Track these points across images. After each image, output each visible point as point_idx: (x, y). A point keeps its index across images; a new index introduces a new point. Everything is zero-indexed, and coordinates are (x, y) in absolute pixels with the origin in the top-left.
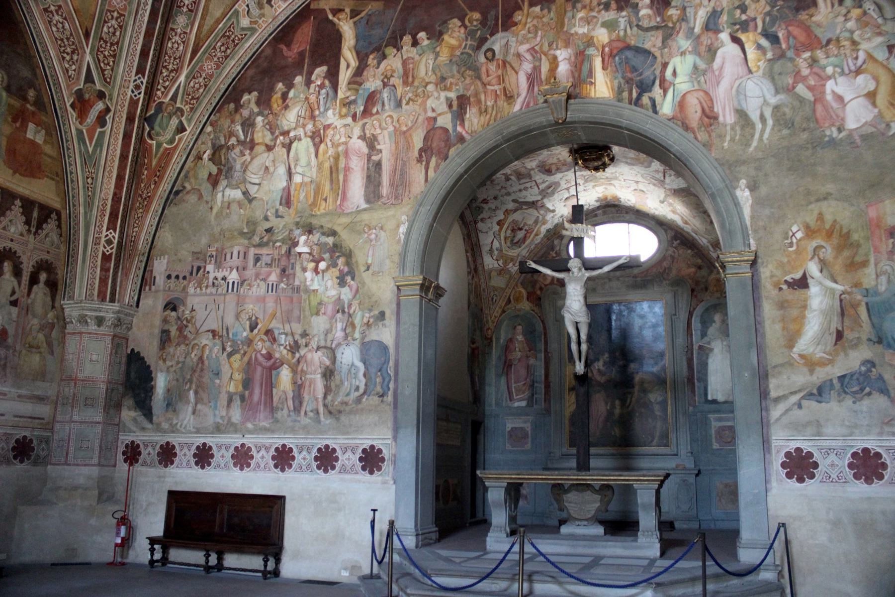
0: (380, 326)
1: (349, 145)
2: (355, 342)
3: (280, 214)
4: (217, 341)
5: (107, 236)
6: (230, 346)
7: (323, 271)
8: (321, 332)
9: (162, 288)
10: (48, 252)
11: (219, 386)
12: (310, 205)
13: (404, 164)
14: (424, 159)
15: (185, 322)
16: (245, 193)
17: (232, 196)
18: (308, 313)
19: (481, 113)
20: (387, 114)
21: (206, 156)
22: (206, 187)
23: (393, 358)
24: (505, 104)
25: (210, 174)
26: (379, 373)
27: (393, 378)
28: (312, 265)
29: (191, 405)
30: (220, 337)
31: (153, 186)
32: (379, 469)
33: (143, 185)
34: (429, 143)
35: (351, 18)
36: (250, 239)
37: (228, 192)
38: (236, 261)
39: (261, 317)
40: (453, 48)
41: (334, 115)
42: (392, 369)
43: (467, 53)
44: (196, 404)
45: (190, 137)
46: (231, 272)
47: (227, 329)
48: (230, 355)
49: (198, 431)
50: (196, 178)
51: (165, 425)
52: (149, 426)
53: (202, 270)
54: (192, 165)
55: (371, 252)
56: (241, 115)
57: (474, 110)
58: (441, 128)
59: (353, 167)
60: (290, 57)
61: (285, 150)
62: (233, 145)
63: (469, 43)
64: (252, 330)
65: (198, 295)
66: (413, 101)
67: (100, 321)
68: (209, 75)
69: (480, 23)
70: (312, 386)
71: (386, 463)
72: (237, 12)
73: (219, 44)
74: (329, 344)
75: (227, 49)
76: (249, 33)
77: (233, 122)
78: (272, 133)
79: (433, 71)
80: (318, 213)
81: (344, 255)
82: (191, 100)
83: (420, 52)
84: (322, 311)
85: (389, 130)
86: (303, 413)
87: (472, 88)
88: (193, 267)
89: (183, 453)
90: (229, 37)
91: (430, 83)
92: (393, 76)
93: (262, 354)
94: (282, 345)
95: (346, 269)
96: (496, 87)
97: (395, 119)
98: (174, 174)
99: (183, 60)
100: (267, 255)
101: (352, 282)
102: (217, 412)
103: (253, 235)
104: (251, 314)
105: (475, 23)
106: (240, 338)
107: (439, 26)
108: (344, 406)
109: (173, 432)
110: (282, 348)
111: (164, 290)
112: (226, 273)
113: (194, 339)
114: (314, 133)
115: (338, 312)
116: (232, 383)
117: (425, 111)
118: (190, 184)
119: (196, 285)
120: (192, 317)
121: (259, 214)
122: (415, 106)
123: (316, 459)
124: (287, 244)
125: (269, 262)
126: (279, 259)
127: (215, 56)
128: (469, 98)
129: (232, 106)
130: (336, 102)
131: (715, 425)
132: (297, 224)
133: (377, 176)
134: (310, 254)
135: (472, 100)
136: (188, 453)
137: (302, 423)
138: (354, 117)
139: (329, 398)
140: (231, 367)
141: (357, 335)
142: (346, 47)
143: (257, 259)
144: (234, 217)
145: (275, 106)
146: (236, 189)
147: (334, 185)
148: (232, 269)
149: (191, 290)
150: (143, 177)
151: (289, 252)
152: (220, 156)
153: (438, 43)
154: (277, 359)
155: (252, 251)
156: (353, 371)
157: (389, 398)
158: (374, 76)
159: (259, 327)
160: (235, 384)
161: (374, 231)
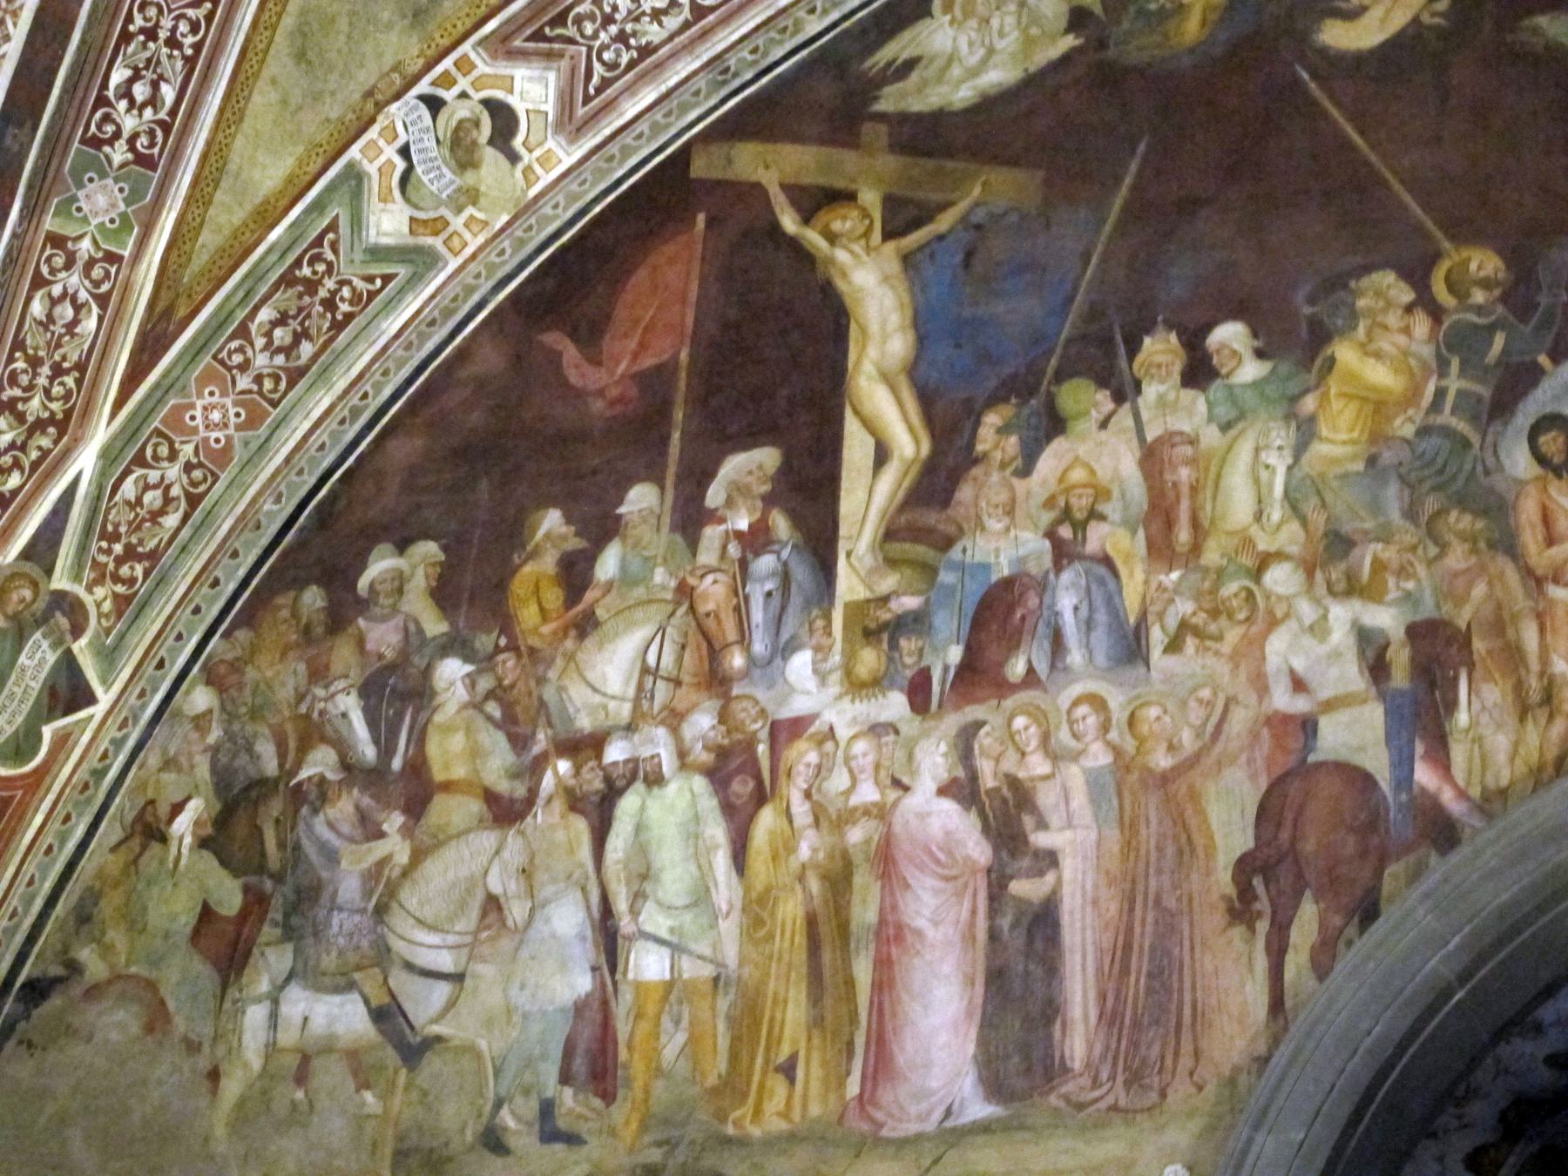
1: (897, 828)
3: (562, 1124)
12: (715, 1092)
13: (1168, 925)
14: (1263, 904)
16: (387, 1015)
17: (318, 1024)
19: (1524, 711)
20: (1077, 689)
21: (183, 826)
25: (207, 914)
34: (1285, 835)
35: (888, 235)
37: (297, 1003)
40: (1378, 406)
41: (821, 676)
43: (1447, 432)
45: (112, 732)
50: (135, 923)
54: (114, 864)
56: (361, 642)
57: (1494, 693)
59: (921, 923)
60: (600, 393)
61: (581, 827)
62: (322, 781)
63: (1454, 384)
66: (1198, 632)
68: (210, 452)
69: (1504, 299)
72: (354, 175)
73: (265, 315)
75: (297, 338)
76: (402, 271)
77: (319, 673)
78: (519, 742)
79: (1292, 502)
80: (755, 1131)
82: (119, 561)
83: (1224, 412)
85: (1088, 763)
87: (1479, 590)
90: (312, 286)
91: (1279, 556)
92: (1102, 518)
97: (1119, 714)
98: (28, 901)
99: (95, 385)
105: (1479, 297)
107: (1312, 300)
114: (722, 753)
117: (1261, 685)
118: (106, 950)
122: (1210, 660)
127: (244, 367)
128: (1464, 640)
129: (313, 598)
130: (828, 618)
133: (1037, 971)
135: (1479, 645)
138: (918, 692)
142: (868, 367)
144: (333, 1128)
145: (528, 615)
146: (337, 990)
147: (828, 1001)
153: (1312, 378)
158: (1010, 510)
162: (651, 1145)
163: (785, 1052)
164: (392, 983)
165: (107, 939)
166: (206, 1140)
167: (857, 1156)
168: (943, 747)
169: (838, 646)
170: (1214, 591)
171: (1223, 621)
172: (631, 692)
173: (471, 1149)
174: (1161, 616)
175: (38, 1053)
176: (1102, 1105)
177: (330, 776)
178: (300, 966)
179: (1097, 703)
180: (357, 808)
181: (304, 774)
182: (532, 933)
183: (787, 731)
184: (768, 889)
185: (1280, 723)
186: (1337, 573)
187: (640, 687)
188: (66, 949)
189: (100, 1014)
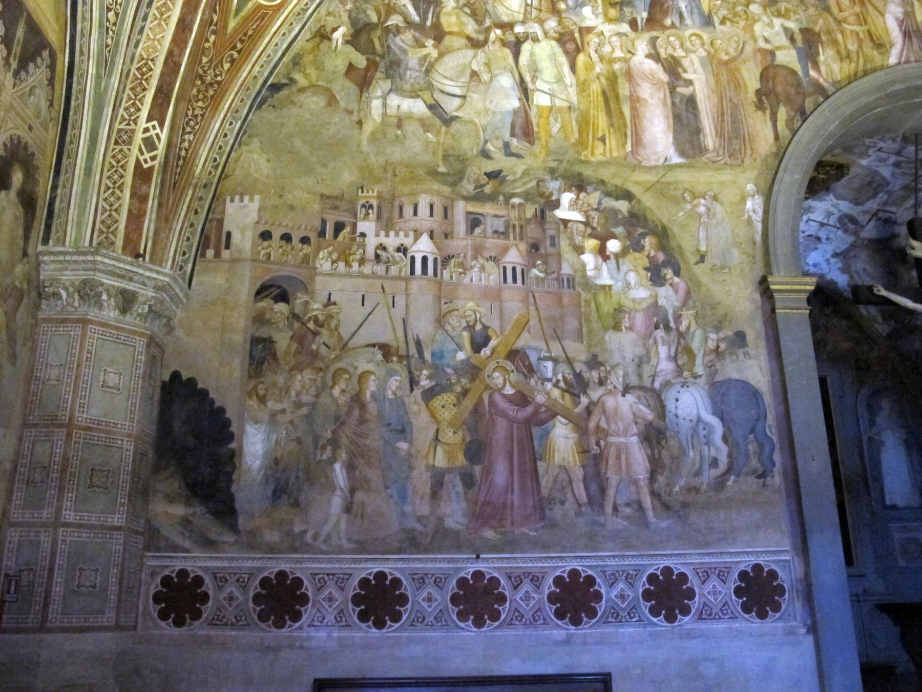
0: (741, 356)
1: (632, 64)
2: (698, 380)
3: (514, 150)
4: (395, 365)
5: (146, 130)
6: (429, 377)
7: (617, 256)
8: (628, 359)
10: (30, 128)
11: (409, 454)
12: (574, 145)
13: (735, 108)
14: (767, 105)
15: (311, 325)
16: (434, 107)
18: (596, 325)
19: (842, 59)
20: (690, 31)
21: (338, 35)
22: (344, 89)
23: (773, 413)
24: (875, 53)
25: (351, 67)
26: (751, 436)
27: (777, 445)
28: (592, 243)
29: (338, 492)
31: (227, 66)
32: (777, 608)
33: (205, 60)
36: (454, 184)
37: (394, 100)
39: (495, 324)
41: (596, 16)
42: (773, 431)
44: (352, 491)
46: (416, 240)
47: (418, 344)
48: (429, 395)
49: (361, 547)
50: (319, 67)
52: (229, 538)
53: (347, 229)
54: (309, 46)
55: (702, 235)
58: (784, 67)
61: (507, 52)
65: (340, 275)
66: (729, 19)
67: (127, 301)
70: (623, 457)
71: (786, 596)
74: (647, 382)
78: (480, 22)
80: (593, 159)
81: (653, 232)
84: (626, 323)
86: (609, 509)
88: (324, 222)
93: (504, 396)
94: (549, 380)
95: (661, 257)
96: (857, 28)
98: (276, 52)
100: (496, 216)
101: (676, 280)
103: (461, 179)
104: (472, 319)
106: (452, 363)
108: (694, 493)
109: (295, 550)
110: (549, 386)
111: (253, 260)
112: (407, 242)
113: (337, 359)
114: (562, 35)
115: (657, 327)
116: (438, 448)
118: (307, 76)
119: (335, 256)
120: (331, 316)
121: (468, 146)
123: (647, 595)
124: (534, 202)
125: (502, 229)
126: (521, 227)
131: (897, 536)
132: (552, 172)
133: (691, 117)
134: (586, 224)
135: (824, 38)
136: (336, 594)
137: (610, 526)
138: (633, 24)
139: (661, 479)
140: (433, 416)
141: (699, 369)
146: (411, 97)
147: (615, 120)
148: (417, 235)
149: (324, 263)
150: (207, 45)
151: (541, 217)
152: (372, 42)
154: (540, 406)
155: (461, 209)
156: (702, 433)
157: (777, 479)
159: (493, 343)
160: (445, 451)
161: (702, 201)
163: (600, 134)
164: (435, 96)
165: (307, 72)
166: (358, 146)
168: (645, 43)
169: (601, 7)
170: (734, 8)
171: (738, 18)
172: (522, 11)
173: (476, 156)
174: (716, 13)
175: (278, 111)
176: (722, 162)
177: (400, 25)
178: (394, 87)
179: (700, 37)
180: (414, 36)
181: (389, 23)
182: (492, 84)
183: (586, 31)
184: (585, 80)
185: (763, 52)
186: (774, 9)
187: (526, 10)
188: (289, 74)
189: (306, 98)
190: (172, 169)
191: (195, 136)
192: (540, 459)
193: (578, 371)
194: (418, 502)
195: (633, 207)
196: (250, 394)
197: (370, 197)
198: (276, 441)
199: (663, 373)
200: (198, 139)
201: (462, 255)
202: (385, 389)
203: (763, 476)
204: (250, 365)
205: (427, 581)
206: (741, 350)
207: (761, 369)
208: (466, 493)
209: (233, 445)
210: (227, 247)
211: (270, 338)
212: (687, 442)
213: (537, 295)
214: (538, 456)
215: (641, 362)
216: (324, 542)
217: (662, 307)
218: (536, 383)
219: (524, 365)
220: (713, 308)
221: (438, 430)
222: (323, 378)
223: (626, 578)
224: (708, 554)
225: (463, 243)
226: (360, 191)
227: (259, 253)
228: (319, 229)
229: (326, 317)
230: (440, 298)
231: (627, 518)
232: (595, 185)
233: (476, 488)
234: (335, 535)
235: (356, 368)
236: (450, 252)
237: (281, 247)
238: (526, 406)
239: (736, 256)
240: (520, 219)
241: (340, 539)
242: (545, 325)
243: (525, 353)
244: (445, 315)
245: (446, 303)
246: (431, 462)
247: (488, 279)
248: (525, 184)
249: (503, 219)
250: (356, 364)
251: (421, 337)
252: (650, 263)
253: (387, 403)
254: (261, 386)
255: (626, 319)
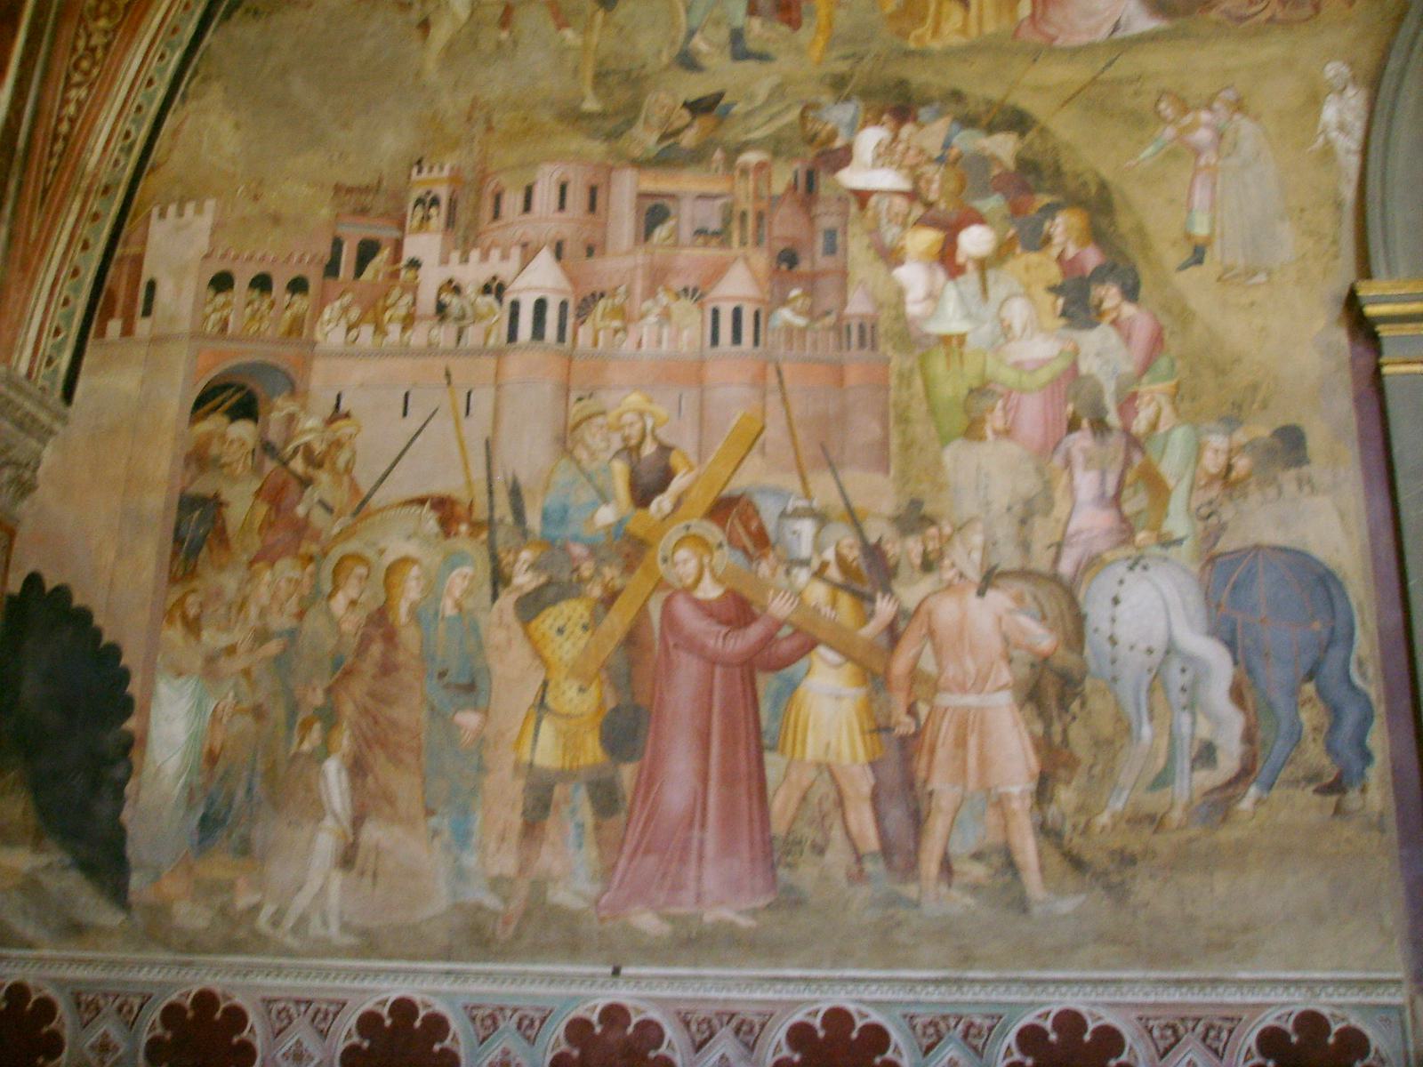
0: (1290, 487)
2: (1172, 552)
3: (752, 45)
4: (463, 541)
6: (534, 566)
7: (983, 265)
9: (185, 326)
15: (298, 465)
18: (921, 429)
23: (1372, 625)
26: (1309, 689)
27: (1380, 710)
28: (927, 239)
29: (329, 822)
30: (476, 527)
36: (613, 136)
38: (547, 219)
39: (686, 442)
44: (358, 821)
46: (525, 264)
47: (515, 493)
48: (531, 606)
49: (370, 944)
51: (191, 915)
53: (385, 254)
55: (1200, 196)
64: (642, 495)
70: (973, 741)
74: (1041, 561)
80: (936, 45)
81: (1074, 201)
84: (996, 420)
86: (930, 864)
88: (337, 245)
89: (289, 1043)
94: (805, 563)
95: (1092, 258)
100: (703, 197)
101: (1128, 310)
102: (470, 860)
103: (630, 123)
104: (634, 432)
108: (1147, 831)
109: (232, 946)
111: (198, 334)
113: (346, 534)
115: (1073, 425)
116: (545, 726)
119: (354, 314)
120: (337, 444)
124: (793, 157)
126: (760, 216)
134: (913, 196)
137: (930, 908)
139: (1066, 796)
141: (1178, 522)
143: (654, 214)
148: (529, 252)
149: (330, 332)
151: (807, 189)
154: (779, 625)
155: (626, 188)
156: (1176, 678)
159: (677, 485)
161: (1205, 116)
162: (837, 59)
166: (418, 75)
167: (1035, 60)
173: (668, 68)
176: (1263, 17)
190: (40, 163)
191: (91, 87)
192: (773, 749)
193: (873, 539)
194: (492, 846)
195: (1030, 146)
196: (169, 616)
197: (436, 181)
198: (215, 711)
199: (1083, 537)
200: (94, 100)
201: (622, 289)
202: (438, 599)
203: (1336, 787)
204: (175, 554)
205: (502, 1025)
206: (1293, 472)
207: (1342, 516)
208: (598, 827)
209: (131, 724)
210: (147, 312)
211: (216, 496)
212: (1138, 706)
213: (786, 368)
214: (766, 741)
215: (1027, 513)
216: (295, 930)
217: (1090, 377)
218: (774, 570)
219: (749, 532)
220: (1220, 371)
221: (545, 684)
222: (315, 575)
223: (966, 1035)
224: (1179, 983)
225: (628, 262)
226: (415, 170)
227: (207, 318)
228: (327, 259)
229: (330, 446)
230: (567, 391)
231: (974, 889)
232: (937, 105)
233: (622, 817)
234: (316, 921)
235: (382, 552)
236: (596, 287)
237: (249, 304)
238: (747, 624)
239: (1288, 243)
240: (757, 196)
241: (325, 923)
242: (801, 434)
243: (750, 503)
244: (577, 425)
245: (580, 399)
246: (526, 757)
247: (675, 339)
248: (771, 118)
249: (719, 202)
250: (382, 545)
251: (523, 478)
252: (1065, 274)
253: (441, 626)
254: (191, 599)
255: (998, 413)
